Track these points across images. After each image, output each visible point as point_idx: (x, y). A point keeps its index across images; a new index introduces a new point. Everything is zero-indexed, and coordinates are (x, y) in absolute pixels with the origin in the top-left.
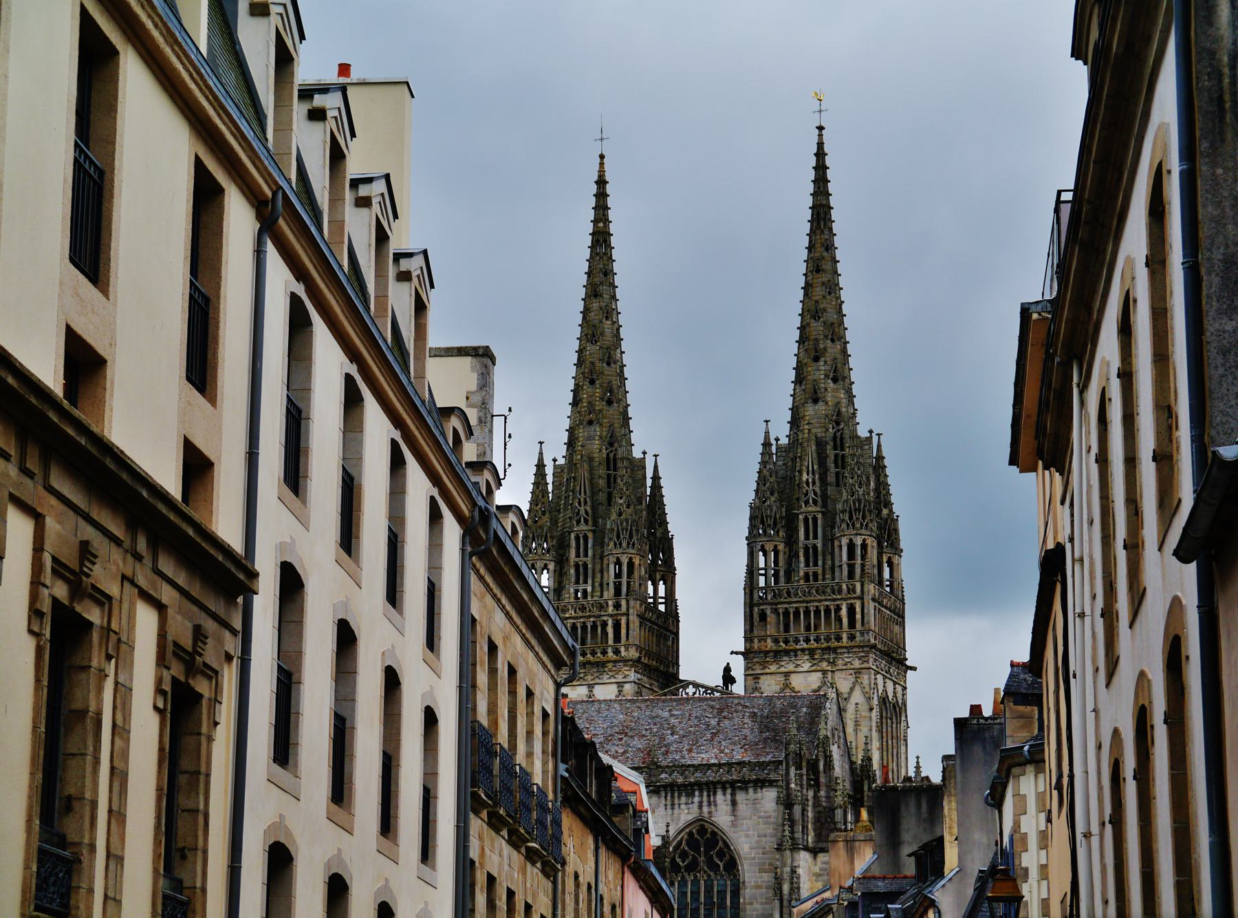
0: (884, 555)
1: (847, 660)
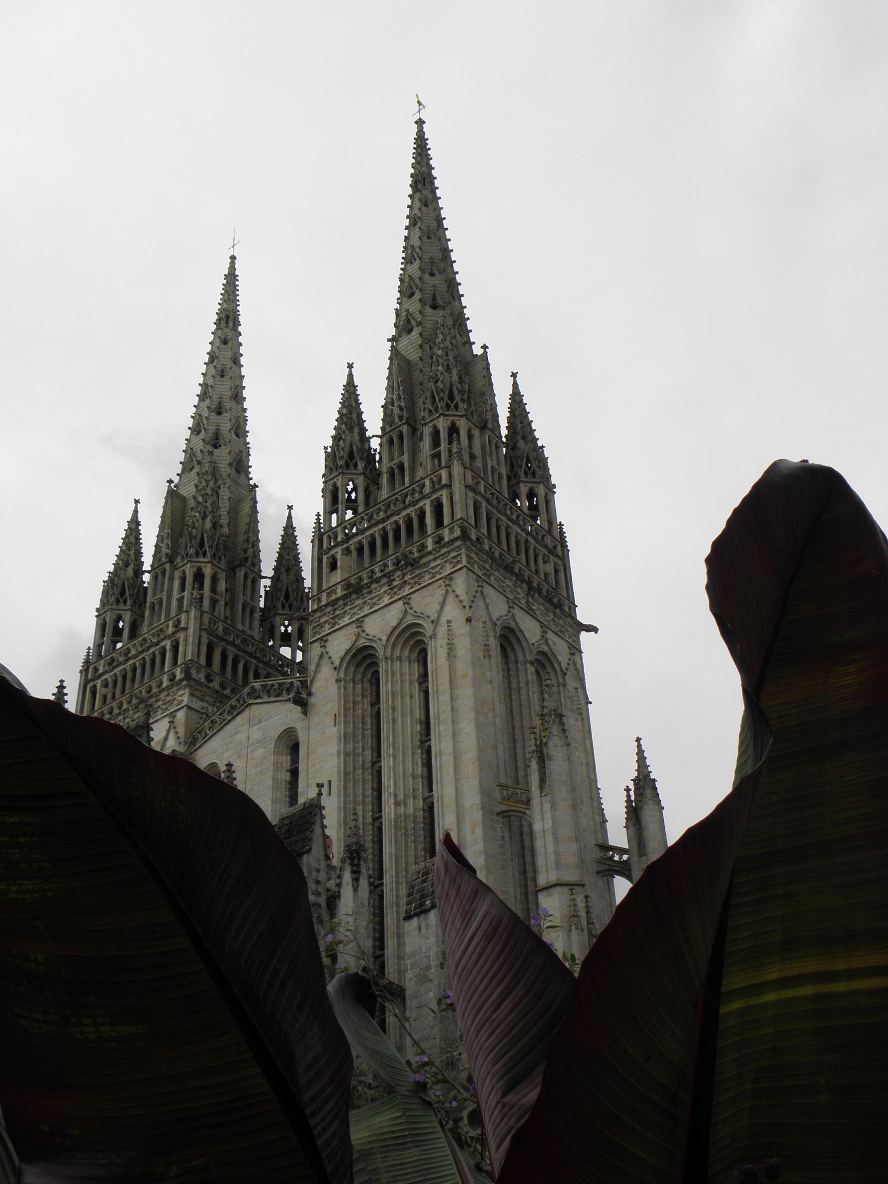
0: (521, 484)
1: (435, 571)
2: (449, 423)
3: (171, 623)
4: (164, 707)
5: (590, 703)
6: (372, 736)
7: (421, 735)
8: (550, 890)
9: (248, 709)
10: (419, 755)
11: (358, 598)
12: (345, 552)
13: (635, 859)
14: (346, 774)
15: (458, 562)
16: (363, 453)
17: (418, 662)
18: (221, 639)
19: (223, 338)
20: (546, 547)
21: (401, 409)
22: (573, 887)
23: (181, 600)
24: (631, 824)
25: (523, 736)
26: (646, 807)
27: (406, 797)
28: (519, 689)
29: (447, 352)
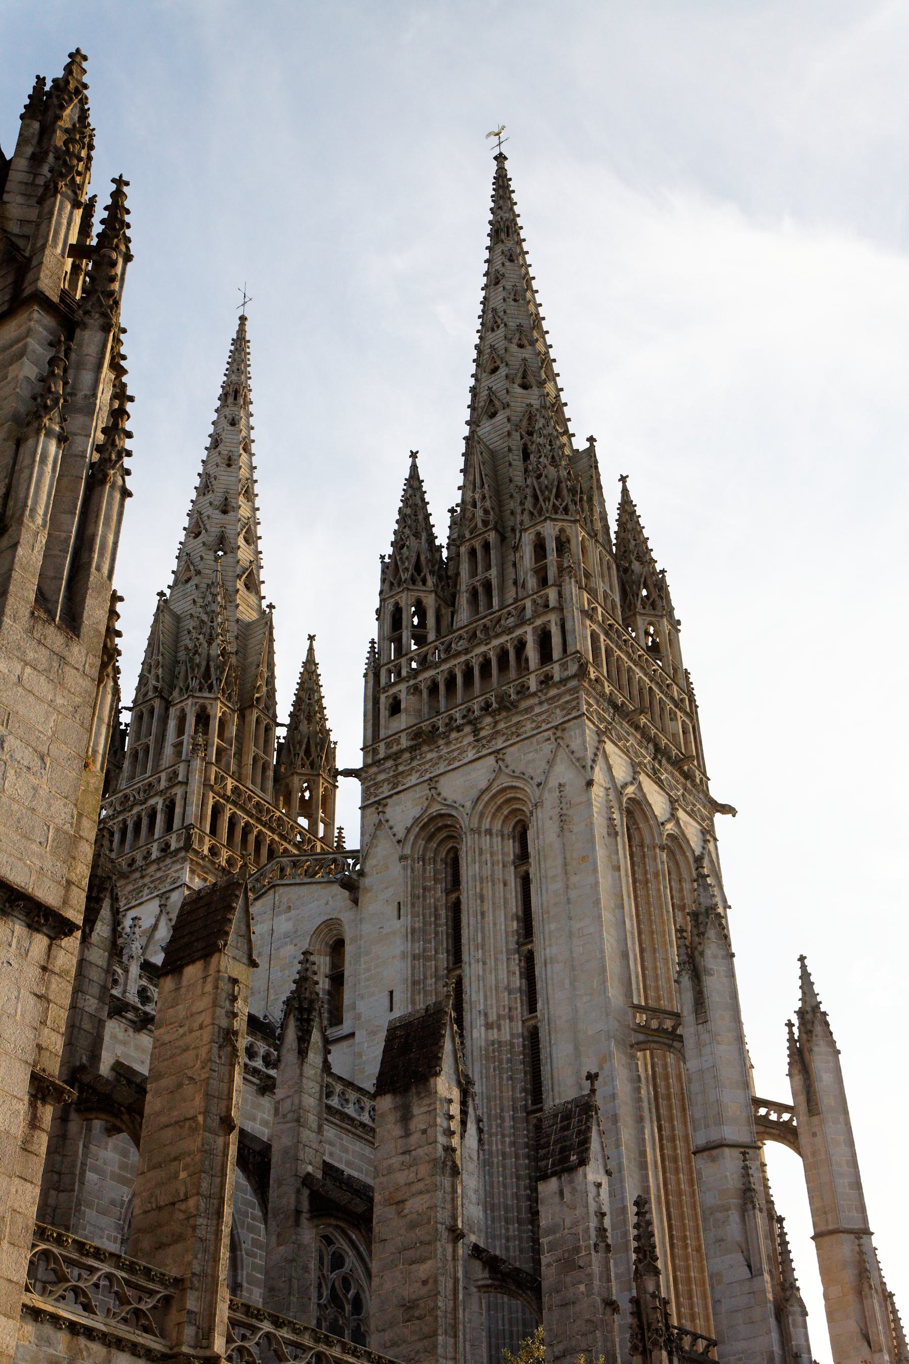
0: (638, 617)
1: (540, 719)
2: (557, 529)
3: (163, 776)
4: (152, 886)
5: (730, 907)
6: (447, 933)
7: (518, 934)
8: (715, 1152)
9: (272, 892)
10: (517, 962)
11: (431, 751)
12: (412, 691)
13: (804, 1118)
14: (414, 983)
15: (574, 708)
16: (433, 566)
17: (514, 838)
18: (227, 799)
19: (230, 417)
20: (672, 699)
21: (486, 512)
22: (747, 1150)
23: (178, 746)
24: (796, 1072)
25: (654, 944)
26: (816, 1049)
27: (499, 1017)
28: (647, 882)
29: (550, 441)
